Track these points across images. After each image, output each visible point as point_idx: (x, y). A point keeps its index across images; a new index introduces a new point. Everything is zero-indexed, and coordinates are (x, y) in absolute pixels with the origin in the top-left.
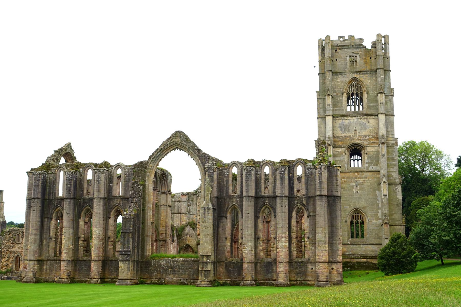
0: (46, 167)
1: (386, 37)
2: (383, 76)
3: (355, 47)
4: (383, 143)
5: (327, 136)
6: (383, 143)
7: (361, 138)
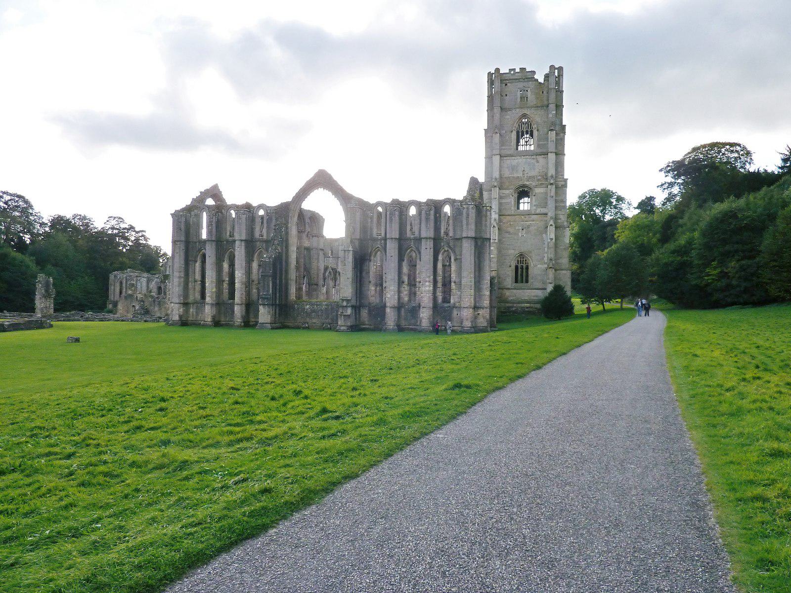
0: (188, 209)
1: (560, 69)
2: (555, 112)
3: (526, 80)
4: (551, 184)
5: (494, 177)
6: (551, 184)
7: (530, 178)
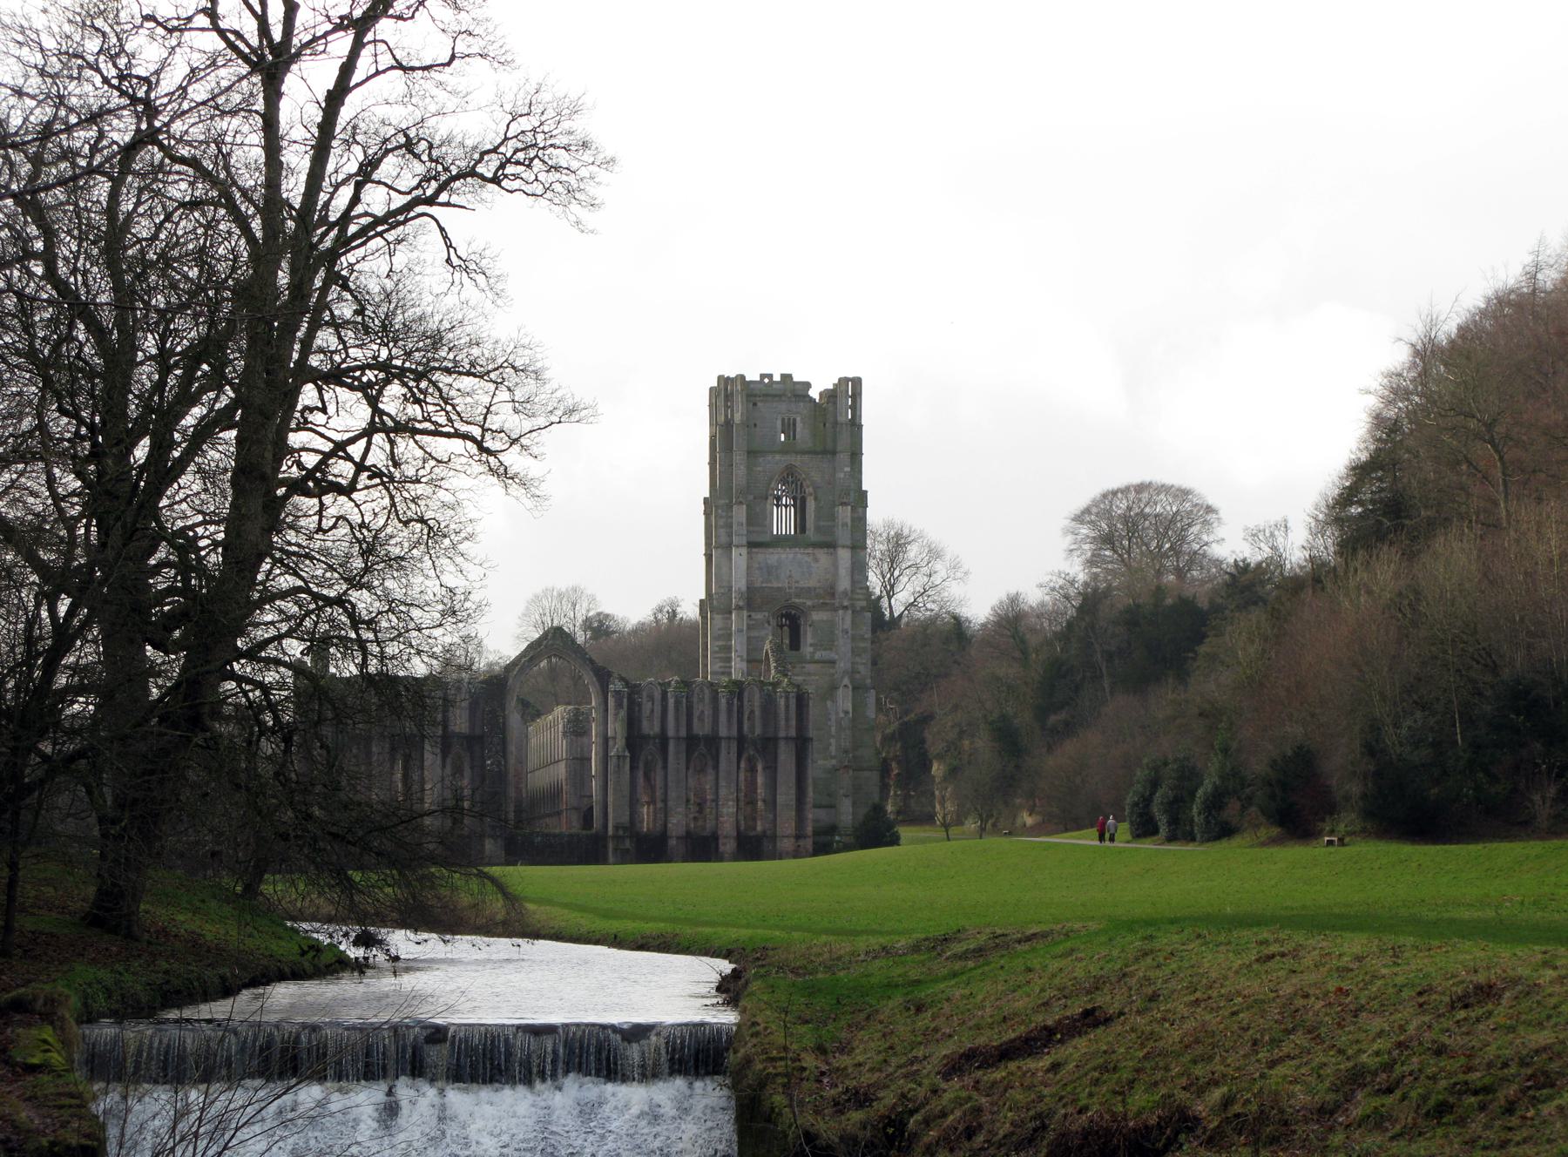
1: (857, 382)
4: (845, 608)
6: (845, 608)
7: (803, 592)
